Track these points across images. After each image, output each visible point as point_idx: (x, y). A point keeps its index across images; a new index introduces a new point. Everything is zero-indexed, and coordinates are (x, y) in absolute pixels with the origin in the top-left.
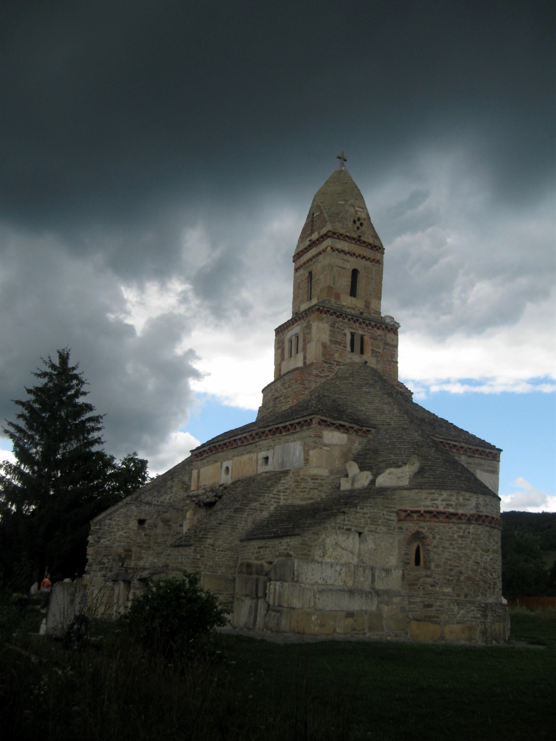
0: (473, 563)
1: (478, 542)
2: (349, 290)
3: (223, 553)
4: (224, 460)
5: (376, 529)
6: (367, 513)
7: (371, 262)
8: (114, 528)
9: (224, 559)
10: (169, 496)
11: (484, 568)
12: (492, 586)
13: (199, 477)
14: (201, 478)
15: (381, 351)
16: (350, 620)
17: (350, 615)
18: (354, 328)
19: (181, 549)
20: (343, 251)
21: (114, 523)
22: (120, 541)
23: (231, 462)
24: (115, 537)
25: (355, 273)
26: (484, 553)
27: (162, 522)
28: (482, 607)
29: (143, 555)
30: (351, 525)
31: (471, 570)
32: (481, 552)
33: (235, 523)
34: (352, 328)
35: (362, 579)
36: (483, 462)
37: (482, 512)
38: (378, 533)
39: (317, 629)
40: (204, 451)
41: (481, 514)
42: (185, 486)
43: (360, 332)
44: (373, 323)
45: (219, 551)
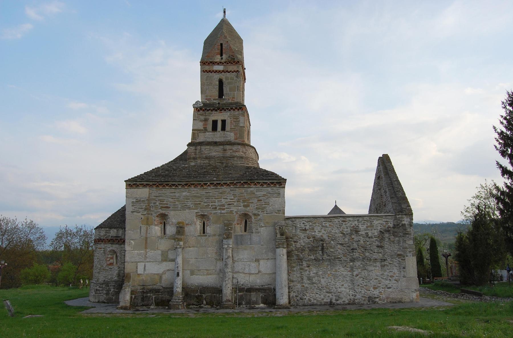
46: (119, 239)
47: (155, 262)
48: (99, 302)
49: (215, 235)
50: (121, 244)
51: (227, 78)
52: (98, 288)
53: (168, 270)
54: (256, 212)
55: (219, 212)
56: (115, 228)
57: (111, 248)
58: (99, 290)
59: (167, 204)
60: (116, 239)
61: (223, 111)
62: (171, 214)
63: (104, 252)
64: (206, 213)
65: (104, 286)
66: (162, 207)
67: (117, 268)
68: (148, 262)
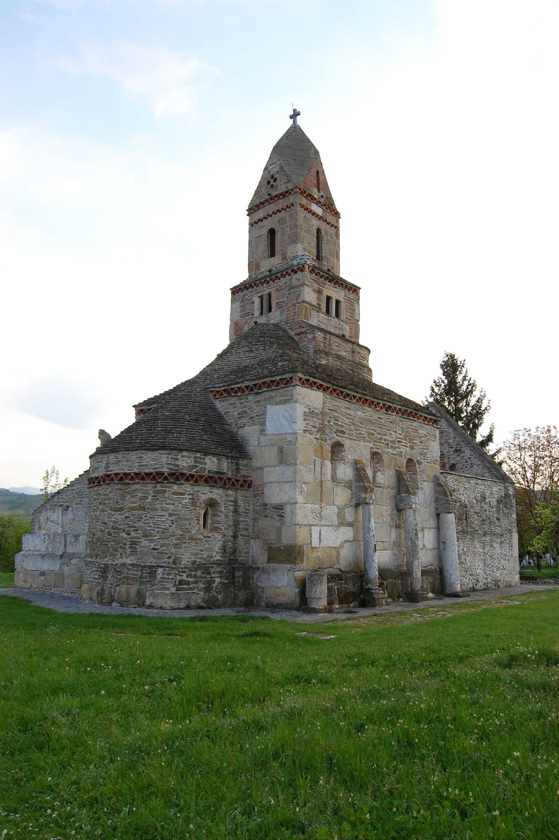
0: (101, 524)
1: (107, 502)
2: (267, 254)
5: (81, 501)
6: (75, 490)
7: (285, 210)
11: (113, 528)
12: (127, 547)
15: (285, 299)
16: (42, 578)
17: (42, 574)
18: (261, 292)
20: (259, 220)
25: (272, 232)
26: (113, 513)
28: (101, 568)
30: (63, 502)
31: (100, 531)
32: (110, 512)
34: (259, 292)
35: (58, 545)
36: (273, 394)
37: (111, 471)
38: (81, 504)
39: (22, 583)
41: (108, 473)
43: (267, 291)
44: (279, 275)
46: (225, 477)
47: (332, 526)
48: (188, 607)
49: (388, 487)
50: (228, 489)
51: (326, 231)
52: (184, 577)
53: (346, 541)
54: (419, 458)
55: (391, 451)
56: (214, 455)
57: (210, 495)
58: (188, 583)
59: (342, 426)
60: (219, 478)
61: (337, 286)
62: (347, 443)
63: (194, 502)
64: (380, 451)
65: (199, 573)
66: (338, 431)
67: (219, 537)
68: (323, 526)
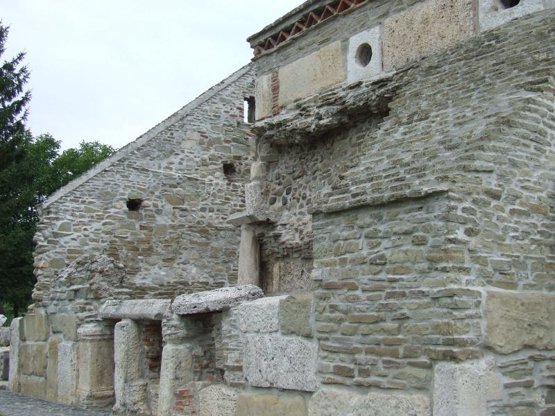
3: (523, 220)
4: (355, 32)
8: (82, 216)
9: (526, 241)
10: (181, 157)
13: (275, 89)
14: (282, 89)
19: (365, 218)
21: (83, 206)
22: (96, 241)
23: (377, 29)
24: (86, 233)
27: (169, 201)
29: (141, 264)
33: (541, 126)
40: (288, 31)
42: (206, 140)
45: (513, 212)
